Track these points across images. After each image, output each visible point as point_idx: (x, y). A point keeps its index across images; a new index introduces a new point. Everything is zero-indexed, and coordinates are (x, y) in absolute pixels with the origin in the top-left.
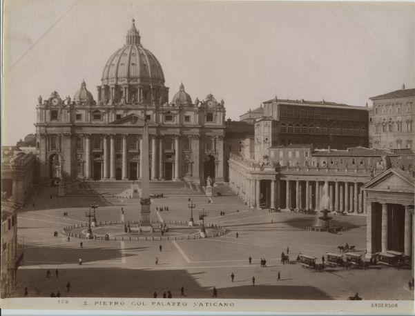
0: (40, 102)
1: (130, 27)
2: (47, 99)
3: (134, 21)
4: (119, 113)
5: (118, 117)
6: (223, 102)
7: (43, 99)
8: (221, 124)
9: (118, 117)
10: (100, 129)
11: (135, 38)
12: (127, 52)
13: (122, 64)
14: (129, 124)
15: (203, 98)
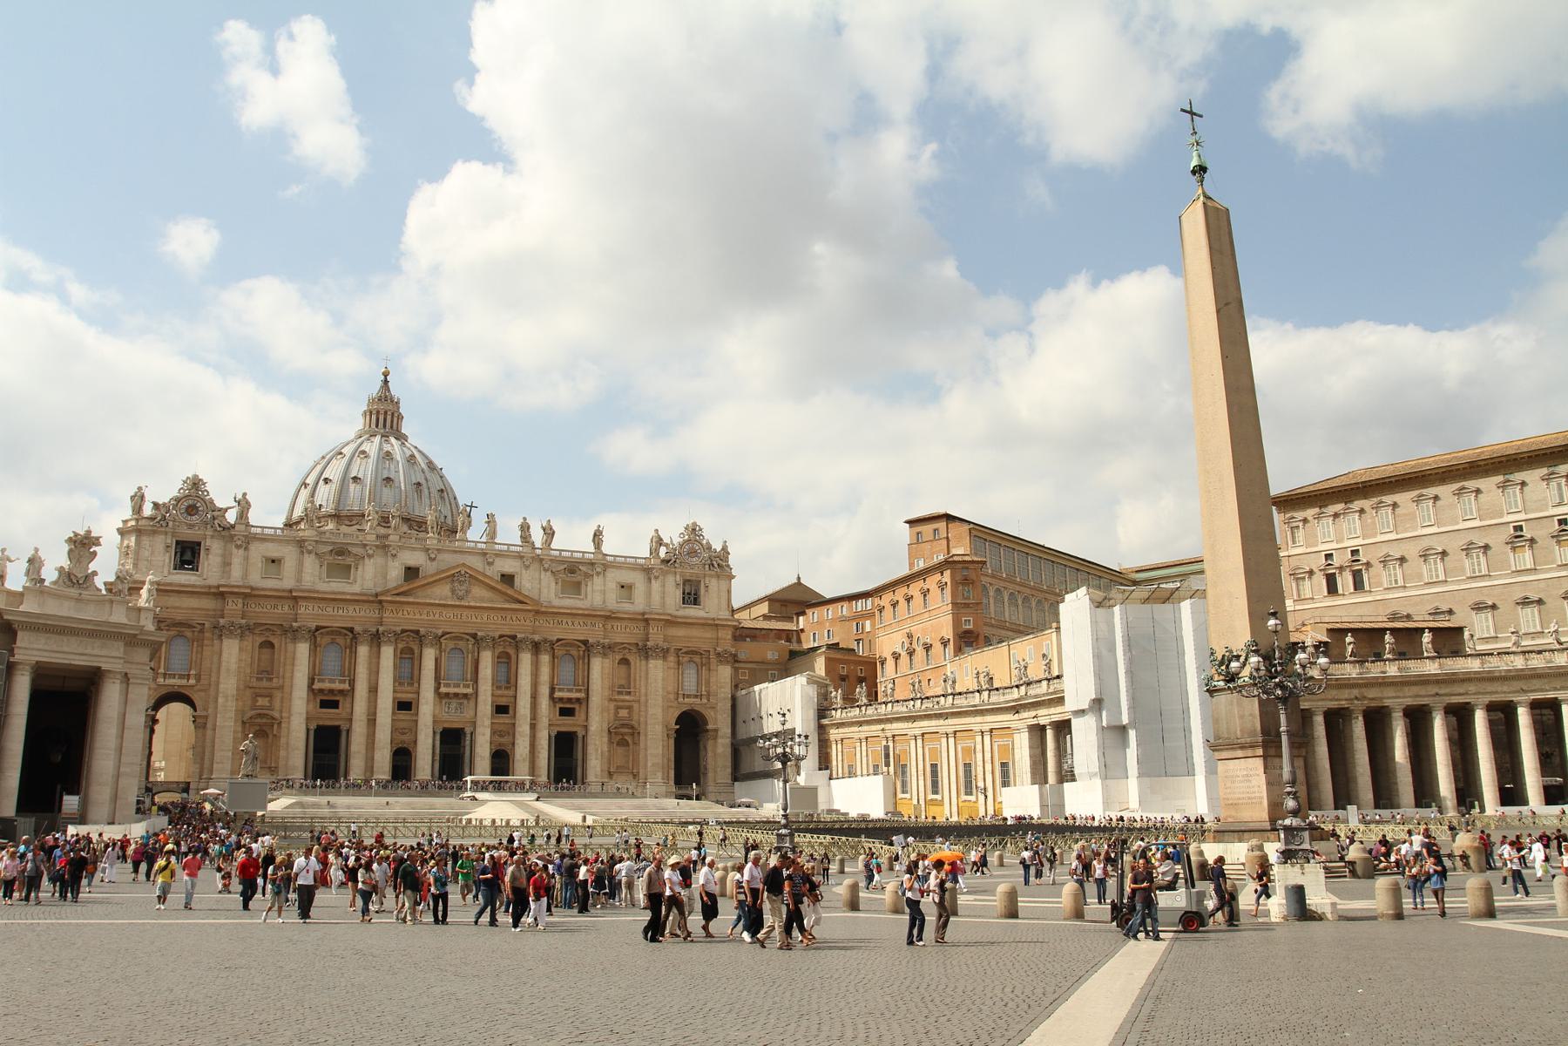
0: (138, 509)
1: (375, 388)
2: (163, 499)
3: (386, 374)
4: (415, 558)
5: (411, 572)
6: (725, 549)
7: (150, 497)
8: (725, 614)
9: (411, 572)
10: (351, 611)
11: (385, 416)
12: (373, 447)
13: (355, 479)
14: (442, 593)
15: (673, 534)
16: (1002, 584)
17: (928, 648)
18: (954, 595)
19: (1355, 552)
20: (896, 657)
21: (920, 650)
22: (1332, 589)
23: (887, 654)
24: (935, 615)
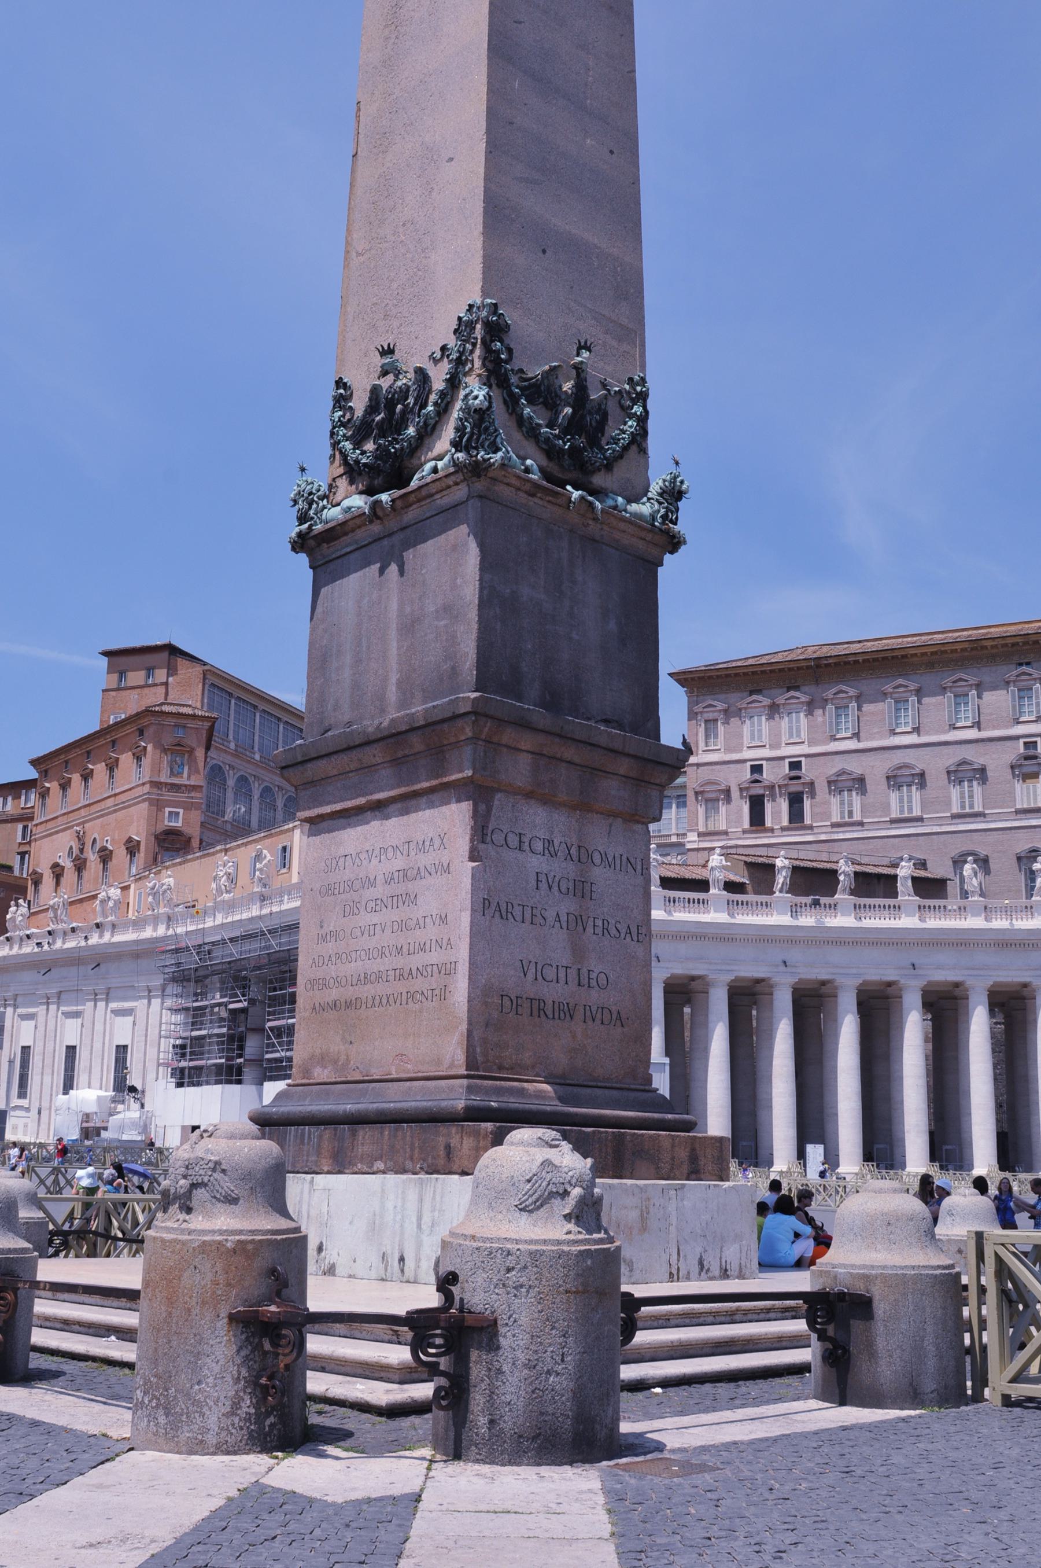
16: (251, 769)
17: (105, 856)
18: (156, 769)
19: (795, 766)
20: (58, 871)
21: (92, 857)
22: (757, 819)
23: (45, 870)
24: (123, 799)
